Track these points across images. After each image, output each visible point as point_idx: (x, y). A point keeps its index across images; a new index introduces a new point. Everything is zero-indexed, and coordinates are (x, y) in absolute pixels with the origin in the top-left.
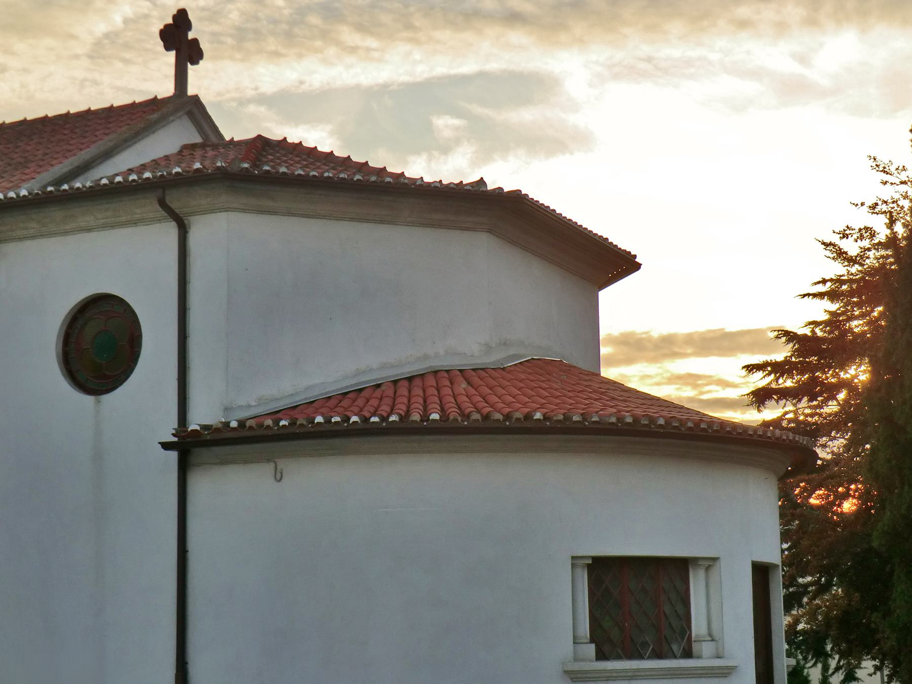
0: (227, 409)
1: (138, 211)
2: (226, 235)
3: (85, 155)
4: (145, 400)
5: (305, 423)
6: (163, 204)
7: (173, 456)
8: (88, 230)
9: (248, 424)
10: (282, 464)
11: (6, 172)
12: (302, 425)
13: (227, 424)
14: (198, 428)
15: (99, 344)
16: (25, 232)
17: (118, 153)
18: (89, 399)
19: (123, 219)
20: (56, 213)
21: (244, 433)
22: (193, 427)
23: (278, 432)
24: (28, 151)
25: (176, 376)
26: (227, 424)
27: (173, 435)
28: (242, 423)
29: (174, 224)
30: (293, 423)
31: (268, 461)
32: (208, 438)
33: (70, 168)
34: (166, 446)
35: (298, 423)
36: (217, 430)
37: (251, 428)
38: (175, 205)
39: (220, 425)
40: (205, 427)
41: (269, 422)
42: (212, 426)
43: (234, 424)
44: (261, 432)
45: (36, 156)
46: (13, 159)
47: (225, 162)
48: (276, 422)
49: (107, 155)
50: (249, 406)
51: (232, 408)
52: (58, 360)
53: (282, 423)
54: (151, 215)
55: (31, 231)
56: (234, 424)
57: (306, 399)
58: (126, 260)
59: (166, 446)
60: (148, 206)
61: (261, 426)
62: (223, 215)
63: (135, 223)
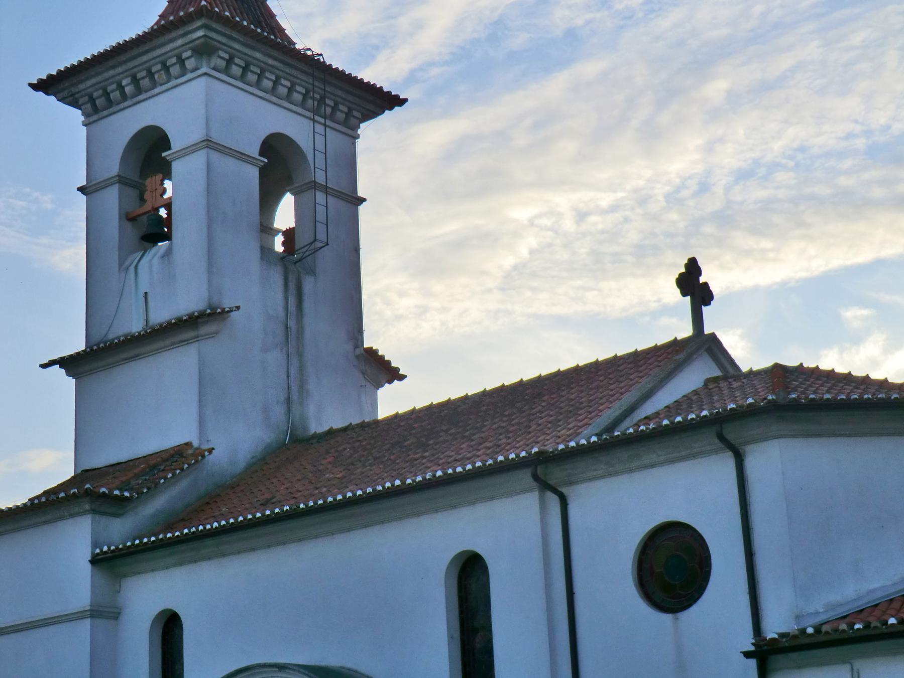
0: (798, 617)
1: (696, 445)
2: (774, 461)
3: (628, 399)
4: (720, 614)
5: (879, 625)
6: (722, 438)
7: (753, 663)
8: (652, 466)
9: (825, 628)
10: (858, 664)
11: (560, 421)
12: (876, 627)
13: (803, 631)
14: (776, 636)
15: (672, 568)
16: (595, 473)
17: (658, 390)
18: (667, 618)
19: (683, 453)
20: (623, 454)
21: (822, 638)
22: (771, 635)
23: (853, 635)
24: (572, 400)
25: (747, 591)
26: (803, 631)
27: (753, 644)
28: (818, 629)
29: (730, 454)
30: (867, 626)
31: (844, 662)
32: (787, 644)
33: (620, 412)
34: (748, 655)
35: (872, 626)
36: (795, 637)
37: (827, 633)
38: (730, 436)
39: (797, 632)
40: (782, 635)
41: (843, 626)
42: (789, 634)
43: (810, 630)
44: (837, 636)
45: (582, 403)
46: (561, 408)
47: (776, 395)
48: (851, 625)
49: (647, 396)
50: (817, 613)
51: (803, 616)
52: (634, 581)
53: (857, 626)
54: (708, 448)
55: (600, 472)
56: (810, 630)
57: (869, 602)
58: (692, 491)
59: (748, 655)
60: (709, 439)
61: (836, 630)
62: (775, 443)
63: (693, 456)
